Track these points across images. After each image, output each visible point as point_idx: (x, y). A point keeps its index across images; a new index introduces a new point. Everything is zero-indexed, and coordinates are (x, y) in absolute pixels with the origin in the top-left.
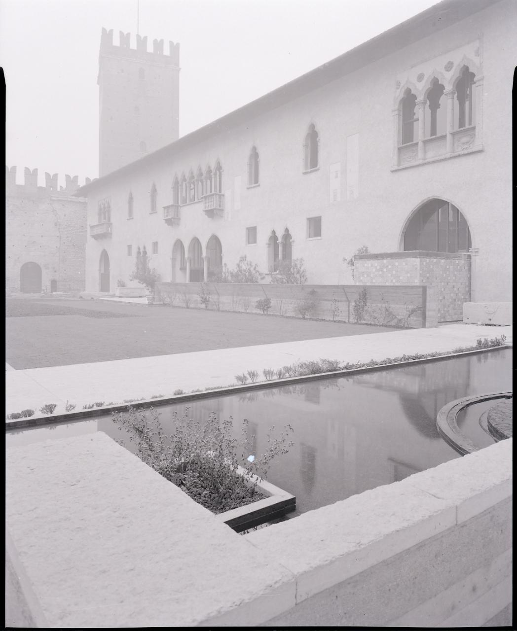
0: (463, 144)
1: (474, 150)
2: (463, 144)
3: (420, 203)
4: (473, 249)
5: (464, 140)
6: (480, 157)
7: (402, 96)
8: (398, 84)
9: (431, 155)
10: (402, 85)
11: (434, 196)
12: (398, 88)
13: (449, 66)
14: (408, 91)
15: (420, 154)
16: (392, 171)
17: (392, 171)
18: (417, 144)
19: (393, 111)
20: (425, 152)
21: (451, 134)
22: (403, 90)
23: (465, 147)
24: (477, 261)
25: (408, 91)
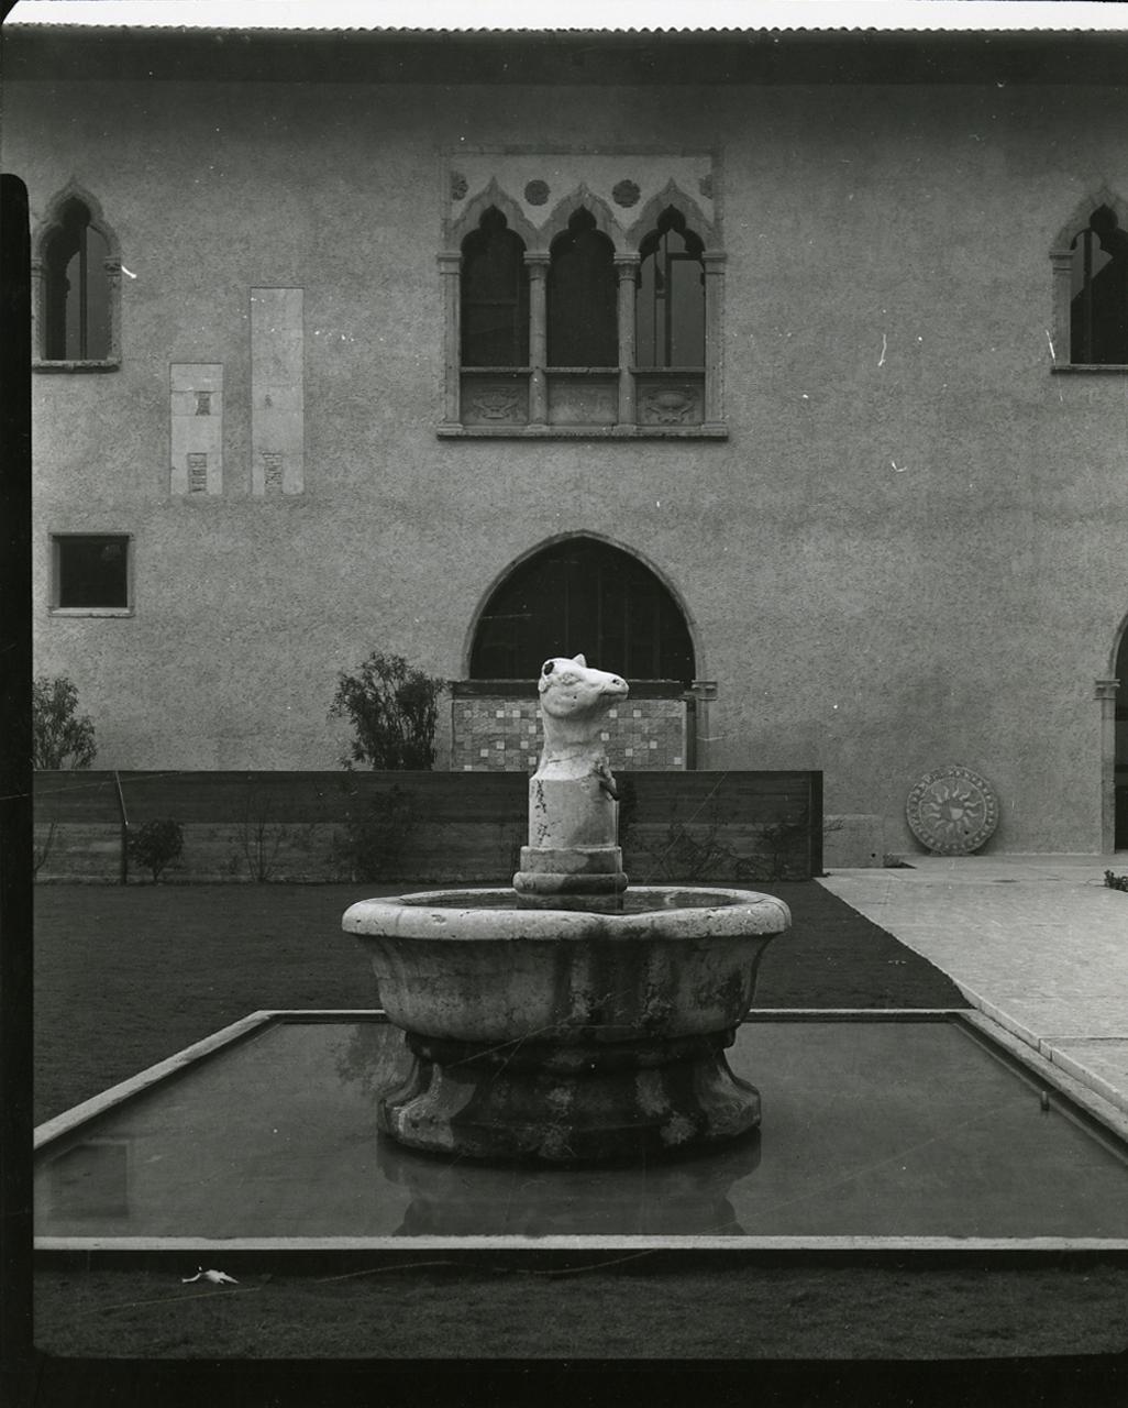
0: (665, 408)
1: (704, 430)
2: (665, 408)
3: (540, 545)
4: (700, 683)
5: (669, 398)
6: (719, 453)
7: (473, 224)
8: (459, 188)
9: (565, 414)
10: (472, 192)
11: (584, 531)
12: (458, 197)
13: (626, 194)
14: (493, 221)
15: (538, 410)
16: (442, 438)
17: (442, 438)
18: (527, 377)
19: (440, 260)
20: (549, 406)
21: (633, 374)
22: (478, 210)
23: (670, 416)
24: (712, 711)
25: (493, 221)
